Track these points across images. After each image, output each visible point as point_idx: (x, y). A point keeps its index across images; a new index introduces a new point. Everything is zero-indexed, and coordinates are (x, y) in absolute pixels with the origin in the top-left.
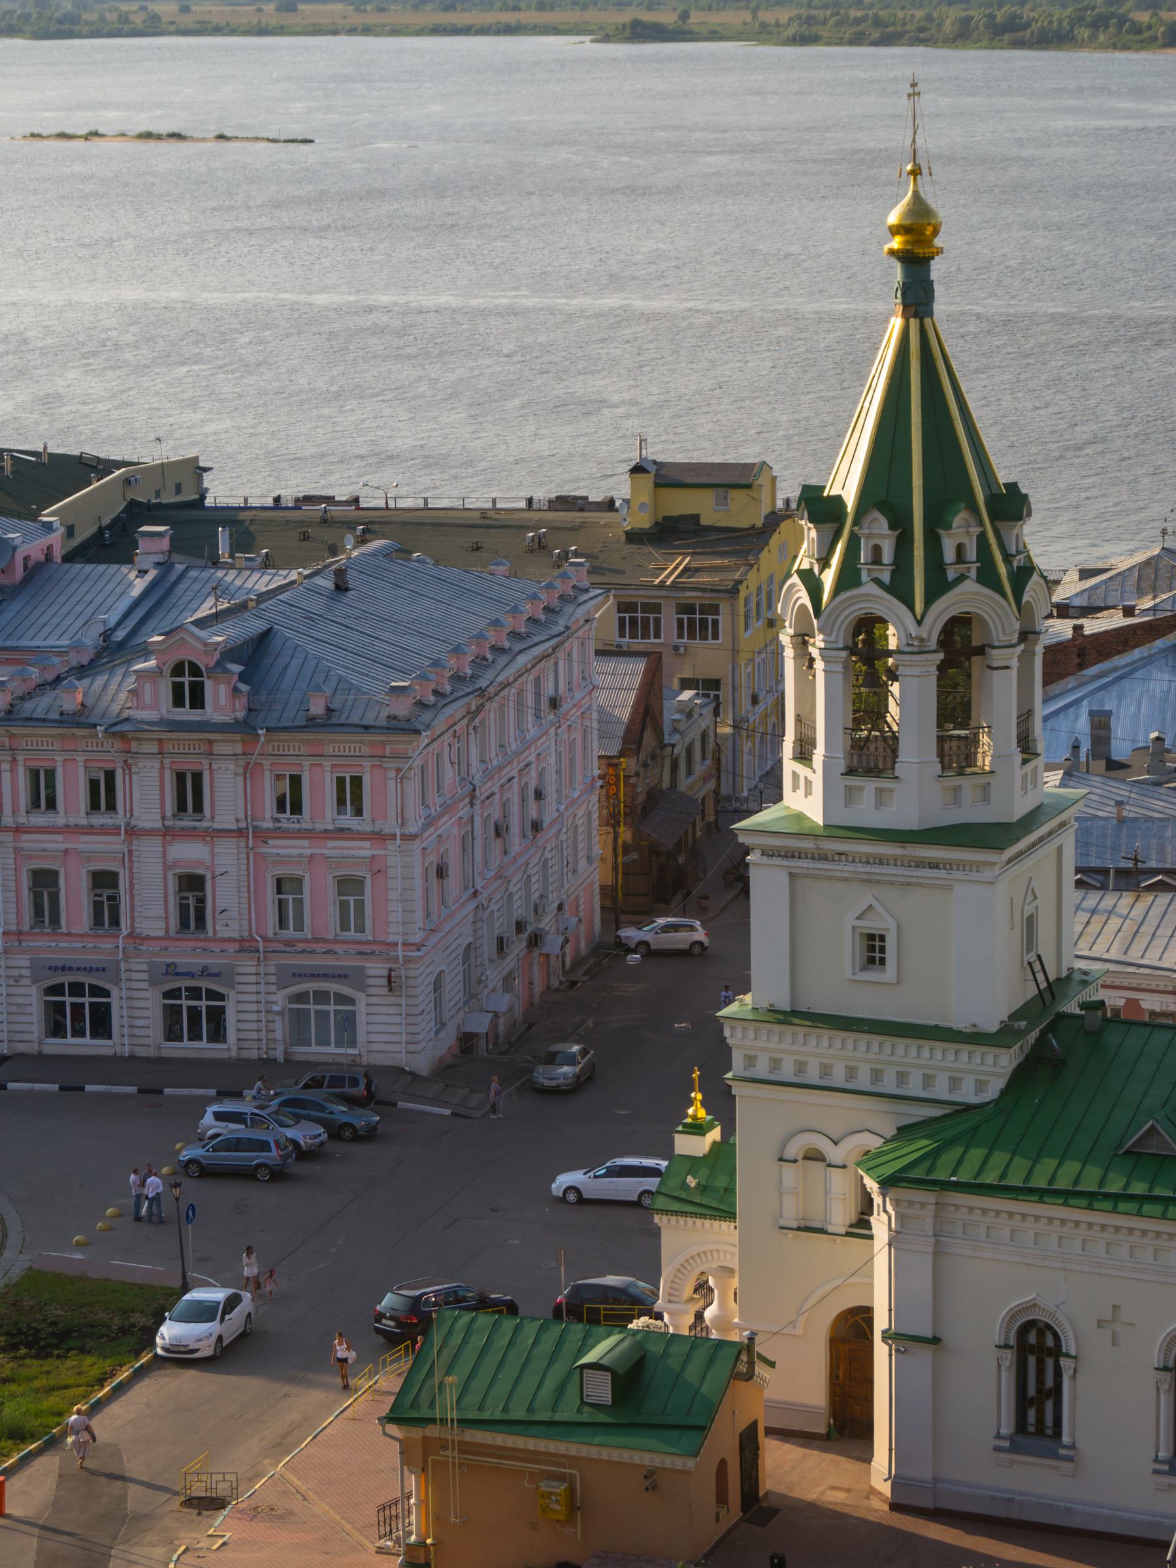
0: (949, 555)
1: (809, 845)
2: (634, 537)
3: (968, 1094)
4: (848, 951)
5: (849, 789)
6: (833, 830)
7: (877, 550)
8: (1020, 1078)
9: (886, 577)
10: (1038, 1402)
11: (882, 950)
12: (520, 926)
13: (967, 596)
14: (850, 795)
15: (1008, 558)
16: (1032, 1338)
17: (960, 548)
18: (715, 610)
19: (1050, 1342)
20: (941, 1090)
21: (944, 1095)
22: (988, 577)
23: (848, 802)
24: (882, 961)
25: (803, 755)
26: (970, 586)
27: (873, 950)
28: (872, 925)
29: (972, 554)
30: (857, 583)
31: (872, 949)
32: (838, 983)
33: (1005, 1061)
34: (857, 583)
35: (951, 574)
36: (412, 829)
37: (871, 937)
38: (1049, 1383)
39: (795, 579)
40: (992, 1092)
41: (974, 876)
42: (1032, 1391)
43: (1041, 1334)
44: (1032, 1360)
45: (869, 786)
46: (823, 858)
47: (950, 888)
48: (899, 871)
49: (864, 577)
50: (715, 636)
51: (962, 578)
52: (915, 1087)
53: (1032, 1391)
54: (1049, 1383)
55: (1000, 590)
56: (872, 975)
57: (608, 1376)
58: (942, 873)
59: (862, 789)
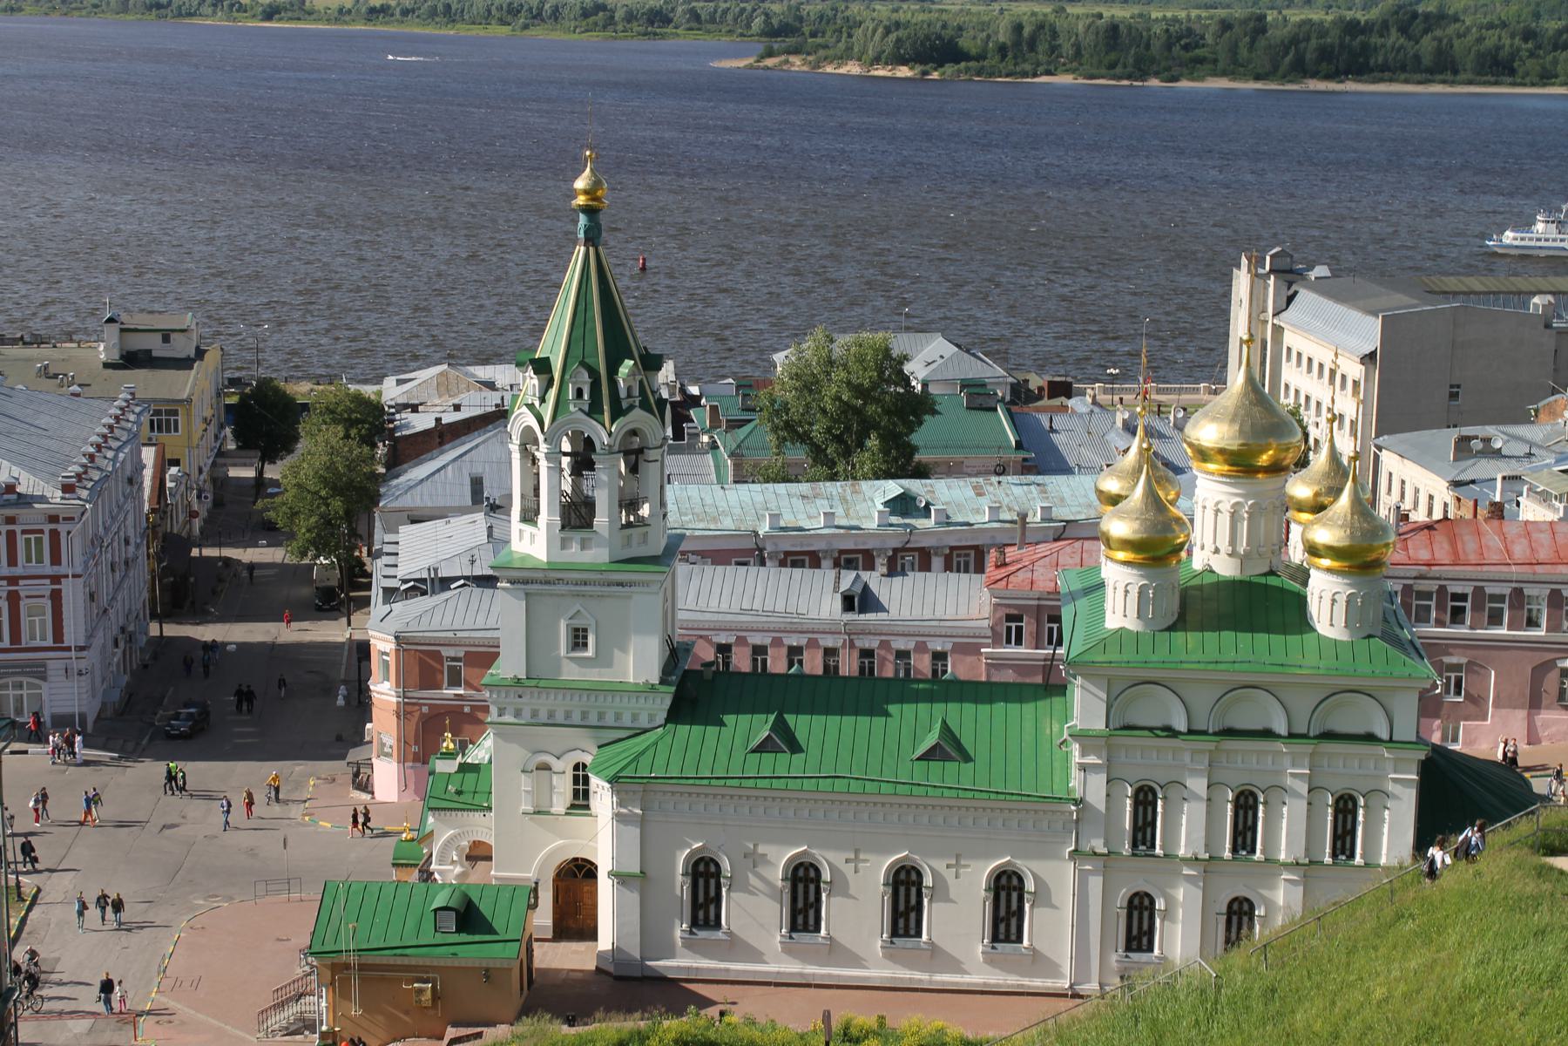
0: (623, 394)
1: (540, 575)
2: (106, 365)
5: (563, 540)
6: (552, 567)
9: (586, 408)
11: (586, 637)
12: (123, 629)
14: (564, 544)
15: (653, 392)
16: (701, 868)
17: (629, 389)
18: (175, 413)
20: (626, 720)
21: (629, 724)
22: (645, 405)
23: (563, 547)
24: (585, 645)
25: (530, 516)
28: (578, 623)
29: (636, 392)
31: (576, 637)
35: (625, 405)
36: (79, 570)
37: (577, 630)
38: (712, 893)
39: (524, 409)
41: (646, 589)
42: (701, 899)
43: (707, 865)
44: (701, 882)
45: (577, 535)
46: (548, 582)
47: (630, 597)
48: (598, 588)
49: (572, 408)
50: (176, 430)
51: (631, 407)
52: (610, 720)
53: (701, 899)
54: (712, 893)
55: (652, 412)
57: (453, 914)
58: (627, 589)
59: (571, 539)
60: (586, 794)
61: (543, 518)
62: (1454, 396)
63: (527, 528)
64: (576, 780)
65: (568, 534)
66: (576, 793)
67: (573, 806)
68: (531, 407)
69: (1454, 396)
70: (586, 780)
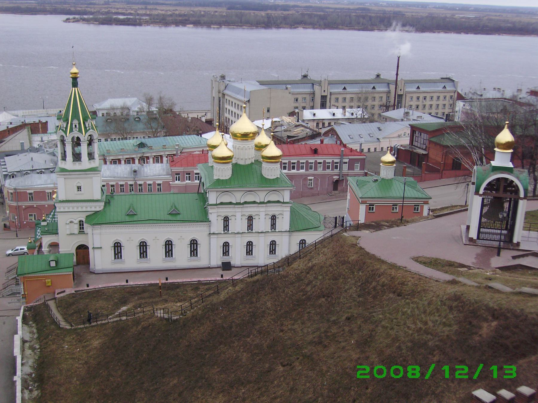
0: (87, 126)
3: (98, 209)
4: (76, 189)
7: (76, 126)
8: (105, 206)
10: (118, 254)
13: (90, 132)
19: (144, 244)
20: (94, 209)
22: (93, 128)
26: (91, 130)
27: (79, 188)
28: (79, 185)
29: (90, 125)
30: (73, 131)
32: (74, 195)
33: (103, 204)
34: (73, 131)
40: (102, 208)
45: (77, 163)
51: (89, 129)
52: (89, 209)
56: (79, 192)
60: (83, 228)
61: (67, 159)
62: (268, 111)
63: (64, 162)
64: (80, 225)
65: (75, 163)
66: (80, 228)
67: (80, 232)
68: (63, 130)
69: (268, 111)
70: (83, 225)
